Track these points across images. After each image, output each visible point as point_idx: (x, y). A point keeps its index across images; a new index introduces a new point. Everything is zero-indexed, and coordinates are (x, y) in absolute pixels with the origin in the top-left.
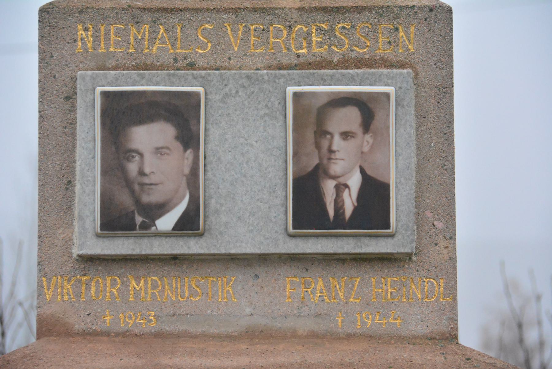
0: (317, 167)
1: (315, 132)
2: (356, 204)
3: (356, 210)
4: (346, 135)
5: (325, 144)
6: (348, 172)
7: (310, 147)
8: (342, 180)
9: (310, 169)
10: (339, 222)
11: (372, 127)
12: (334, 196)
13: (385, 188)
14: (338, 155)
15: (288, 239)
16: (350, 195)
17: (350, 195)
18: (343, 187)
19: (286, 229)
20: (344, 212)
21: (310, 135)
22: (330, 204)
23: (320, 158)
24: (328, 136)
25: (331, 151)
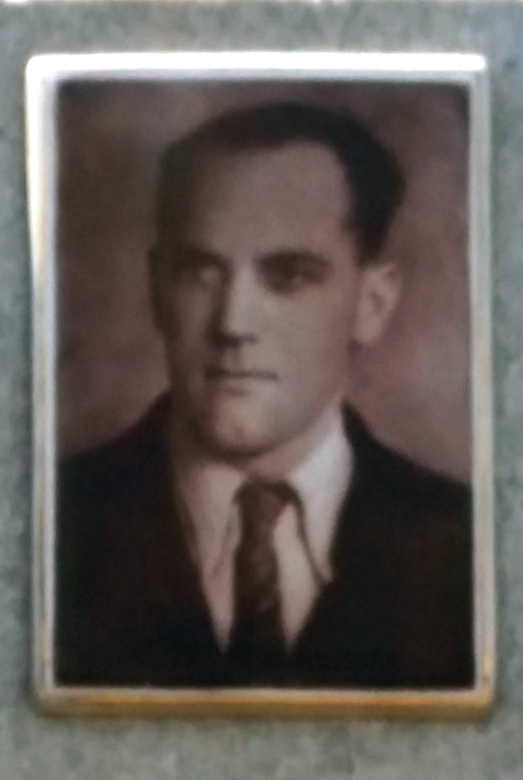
0: (164, 406)
1: (154, 257)
2: (327, 573)
3: (329, 601)
4: (285, 270)
5: (196, 309)
6: (293, 431)
7: (131, 320)
8: (266, 466)
9: (132, 416)
10: (258, 653)
11: (397, 234)
12: (235, 540)
13: (451, 499)
14: (252, 357)
15: (33, 725)
16: (302, 532)
17: (302, 532)
18: (271, 498)
19: (27, 686)
20: (275, 611)
21: (131, 268)
22: (217, 571)
23: (177, 372)
24: (210, 275)
25: (221, 338)
